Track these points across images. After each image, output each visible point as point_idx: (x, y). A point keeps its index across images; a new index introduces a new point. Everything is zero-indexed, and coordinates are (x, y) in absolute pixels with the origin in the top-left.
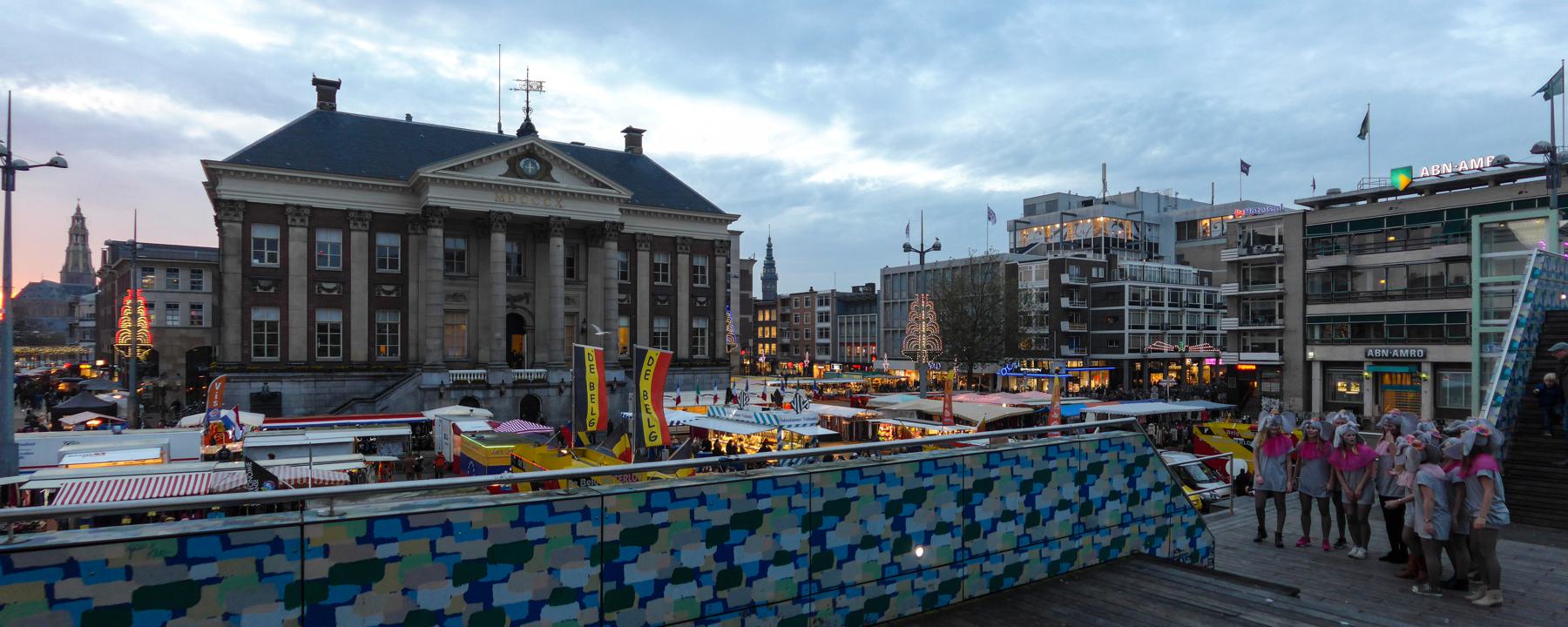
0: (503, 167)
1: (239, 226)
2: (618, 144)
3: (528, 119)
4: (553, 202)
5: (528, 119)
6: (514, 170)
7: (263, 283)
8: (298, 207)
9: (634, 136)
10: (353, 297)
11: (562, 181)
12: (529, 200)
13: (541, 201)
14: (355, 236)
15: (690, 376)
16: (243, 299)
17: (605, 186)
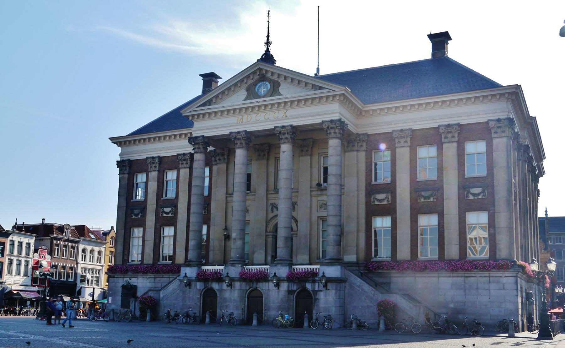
0: (243, 93)
1: (126, 176)
2: (424, 52)
3: (268, 51)
4: (280, 114)
5: (268, 51)
6: (252, 93)
7: (136, 211)
8: (153, 158)
9: (440, 40)
10: (179, 217)
11: (287, 91)
12: (262, 116)
13: (271, 115)
14: (182, 171)
15: (460, 280)
16: (126, 223)
17: (320, 88)
